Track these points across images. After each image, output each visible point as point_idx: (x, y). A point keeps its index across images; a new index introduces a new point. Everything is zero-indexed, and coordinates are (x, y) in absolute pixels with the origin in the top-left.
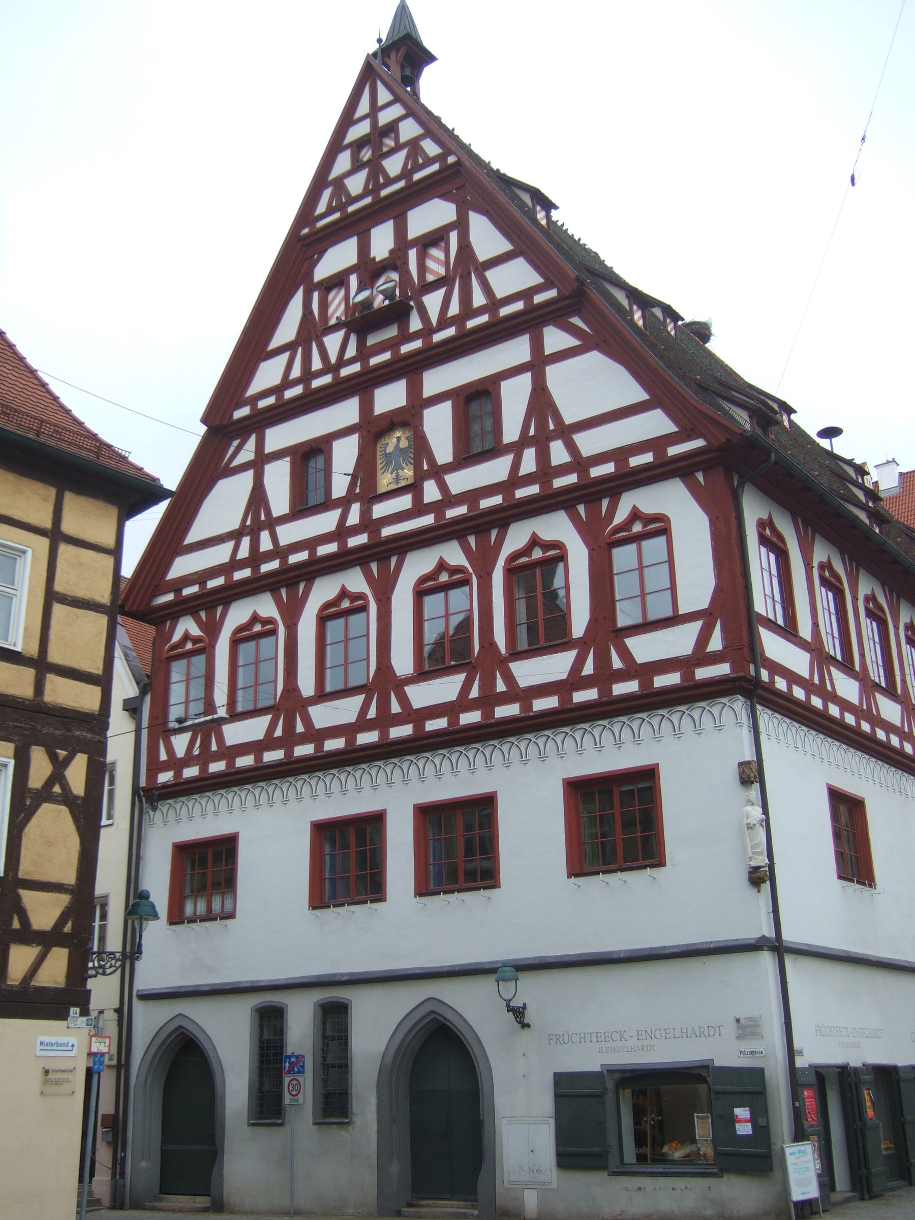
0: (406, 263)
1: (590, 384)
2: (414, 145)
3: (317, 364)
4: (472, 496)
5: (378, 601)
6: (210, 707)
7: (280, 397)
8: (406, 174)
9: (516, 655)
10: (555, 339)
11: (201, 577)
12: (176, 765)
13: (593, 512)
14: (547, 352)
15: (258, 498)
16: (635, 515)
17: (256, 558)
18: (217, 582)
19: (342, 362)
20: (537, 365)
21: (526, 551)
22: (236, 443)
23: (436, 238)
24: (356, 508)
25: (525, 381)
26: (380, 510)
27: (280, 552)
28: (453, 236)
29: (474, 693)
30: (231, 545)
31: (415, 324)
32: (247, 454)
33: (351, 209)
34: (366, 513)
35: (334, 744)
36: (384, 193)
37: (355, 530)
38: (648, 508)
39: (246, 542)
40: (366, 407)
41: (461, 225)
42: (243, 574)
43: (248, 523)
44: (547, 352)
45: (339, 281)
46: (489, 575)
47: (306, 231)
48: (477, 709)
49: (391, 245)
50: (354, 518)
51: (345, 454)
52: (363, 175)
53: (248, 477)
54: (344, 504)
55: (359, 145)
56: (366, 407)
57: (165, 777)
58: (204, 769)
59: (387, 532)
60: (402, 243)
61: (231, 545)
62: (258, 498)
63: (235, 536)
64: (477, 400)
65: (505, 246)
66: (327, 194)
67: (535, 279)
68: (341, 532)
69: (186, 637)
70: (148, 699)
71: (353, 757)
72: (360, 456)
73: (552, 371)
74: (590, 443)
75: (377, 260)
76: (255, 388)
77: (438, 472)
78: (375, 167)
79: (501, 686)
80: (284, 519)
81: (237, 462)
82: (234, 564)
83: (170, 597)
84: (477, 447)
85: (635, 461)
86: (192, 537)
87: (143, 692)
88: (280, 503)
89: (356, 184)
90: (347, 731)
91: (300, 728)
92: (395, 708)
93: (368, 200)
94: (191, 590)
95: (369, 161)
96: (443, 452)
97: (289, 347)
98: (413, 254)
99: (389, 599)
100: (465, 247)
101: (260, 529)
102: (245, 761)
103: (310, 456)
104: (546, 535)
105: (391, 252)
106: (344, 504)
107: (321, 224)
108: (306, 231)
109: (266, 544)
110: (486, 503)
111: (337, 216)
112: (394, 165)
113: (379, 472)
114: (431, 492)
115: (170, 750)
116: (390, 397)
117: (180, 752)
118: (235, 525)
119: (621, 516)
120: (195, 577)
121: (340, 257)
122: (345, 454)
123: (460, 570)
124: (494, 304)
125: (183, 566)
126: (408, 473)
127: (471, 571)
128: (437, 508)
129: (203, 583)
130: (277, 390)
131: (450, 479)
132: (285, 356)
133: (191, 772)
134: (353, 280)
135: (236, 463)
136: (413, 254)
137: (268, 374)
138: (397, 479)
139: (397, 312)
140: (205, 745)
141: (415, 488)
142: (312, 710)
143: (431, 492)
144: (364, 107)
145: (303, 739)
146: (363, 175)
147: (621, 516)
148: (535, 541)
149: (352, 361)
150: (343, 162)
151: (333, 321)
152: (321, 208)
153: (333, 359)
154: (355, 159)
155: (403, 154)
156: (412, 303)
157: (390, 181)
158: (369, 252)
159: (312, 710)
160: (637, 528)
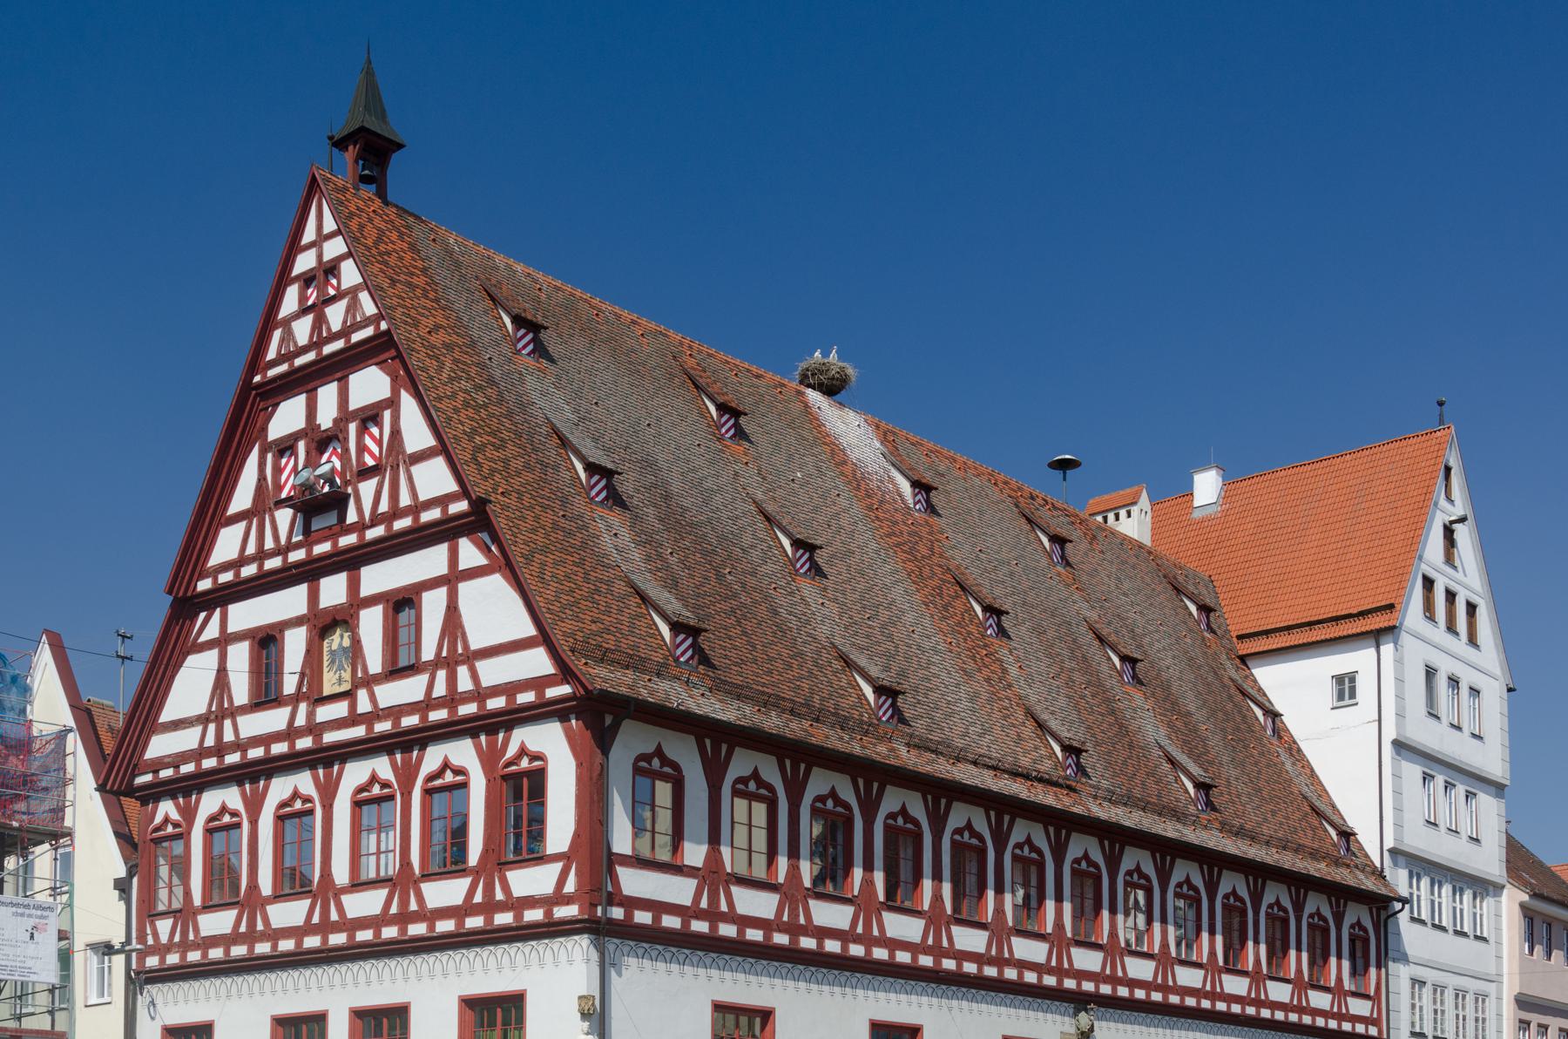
0: (346, 439)
1: (494, 611)
2: (353, 292)
3: (269, 544)
4: (396, 712)
5: (324, 806)
6: (188, 894)
7: (237, 574)
8: (345, 332)
9: (427, 876)
10: (470, 554)
11: (177, 760)
12: (162, 950)
13: (492, 745)
14: (462, 567)
15: (222, 682)
16: (523, 751)
17: (220, 750)
19: (291, 547)
20: (453, 578)
22: (203, 615)
23: (370, 416)
24: (303, 707)
25: (441, 593)
26: (325, 713)
27: (240, 746)
28: (387, 414)
29: (394, 910)
30: (199, 729)
32: (212, 632)
33: (299, 362)
34: (311, 715)
35: (287, 945)
36: (328, 349)
37: (301, 732)
38: (533, 747)
39: (212, 727)
40: (313, 596)
41: (393, 403)
42: (209, 763)
44: (462, 567)
45: (285, 447)
46: (410, 793)
47: (257, 379)
48: (395, 924)
50: (301, 721)
51: (295, 644)
52: (308, 320)
53: (212, 656)
54: (295, 699)
56: (313, 596)
57: (152, 962)
58: (183, 957)
59: (330, 737)
61: (199, 729)
62: (222, 682)
63: (203, 720)
65: (430, 441)
66: (277, 334)
67: (452, 487)
68: (290, 734)
69: (166, 820)
70: (135, 880)
71: (300, 960)
72: (308, 651)
73: (464, 588)
74: (493, 672)
76: (215, 559)
77: (369, 682)
78: (317, 310)
79: (413, 906)
80: (244, 710)
81: (202, 639)
82: (200, 753)
83: (147, 778)
84: (403, 661)
86: (165, 717)
87: (130, 875)
88: (241, 692)
89: (302, 330)
90: (297, 933)
91: (260, 926)
92: (334, 916)
93: (311, 356)
94: (166, 773)
95: (314, 305)
96: (375, 664)
98: (353, 428)
99: (331, 806)
100: (396, 433)
101: (223, 718)
102: (216, 953)
104: (456, 761)
105: (335, 421)
106: (295, 699)
107: (272, 373)
108: (257, 379)
109: (229, 736)
110: (410, 721)
111: (284, 368)
112: (336, 315)
113: (325, 670)
114: (364, 705)
115: (156, 935)
116: (333, 590)
117: (164, 939)
118: (203, 710)
119: (512, 751)
121: (287, 418)
122: (295, 644)
123: (385, 785)
124: (417, 508)
125: (159, 746)
126: (347, 675)
128: (370, 719)
129: (177, 767)
131: (378, 689)
132: (243, 524)
133: (173, 959)
134: (301, 446)
135: (202, 639)
136: (353, 428)
137: (227, 544)
138: (340, 680)
139: (337, 501)
140: (184, 933)
141: (349, 695)
142: (270, 909)
144: (309, 235)
145: (264, 937)
146: (308, 320)
147: (512, 751)
148: (446, 765)
149: (298, 546)
150: (290, 301)
151: (284, 495)
152: (271, 354)
153: (283, 541)
154: (303, 298)
155: (343, 304)
156: (350, 490)
157: (333, 337)
158: (315, 417)
159: (270, 909)
160: (525, 763)
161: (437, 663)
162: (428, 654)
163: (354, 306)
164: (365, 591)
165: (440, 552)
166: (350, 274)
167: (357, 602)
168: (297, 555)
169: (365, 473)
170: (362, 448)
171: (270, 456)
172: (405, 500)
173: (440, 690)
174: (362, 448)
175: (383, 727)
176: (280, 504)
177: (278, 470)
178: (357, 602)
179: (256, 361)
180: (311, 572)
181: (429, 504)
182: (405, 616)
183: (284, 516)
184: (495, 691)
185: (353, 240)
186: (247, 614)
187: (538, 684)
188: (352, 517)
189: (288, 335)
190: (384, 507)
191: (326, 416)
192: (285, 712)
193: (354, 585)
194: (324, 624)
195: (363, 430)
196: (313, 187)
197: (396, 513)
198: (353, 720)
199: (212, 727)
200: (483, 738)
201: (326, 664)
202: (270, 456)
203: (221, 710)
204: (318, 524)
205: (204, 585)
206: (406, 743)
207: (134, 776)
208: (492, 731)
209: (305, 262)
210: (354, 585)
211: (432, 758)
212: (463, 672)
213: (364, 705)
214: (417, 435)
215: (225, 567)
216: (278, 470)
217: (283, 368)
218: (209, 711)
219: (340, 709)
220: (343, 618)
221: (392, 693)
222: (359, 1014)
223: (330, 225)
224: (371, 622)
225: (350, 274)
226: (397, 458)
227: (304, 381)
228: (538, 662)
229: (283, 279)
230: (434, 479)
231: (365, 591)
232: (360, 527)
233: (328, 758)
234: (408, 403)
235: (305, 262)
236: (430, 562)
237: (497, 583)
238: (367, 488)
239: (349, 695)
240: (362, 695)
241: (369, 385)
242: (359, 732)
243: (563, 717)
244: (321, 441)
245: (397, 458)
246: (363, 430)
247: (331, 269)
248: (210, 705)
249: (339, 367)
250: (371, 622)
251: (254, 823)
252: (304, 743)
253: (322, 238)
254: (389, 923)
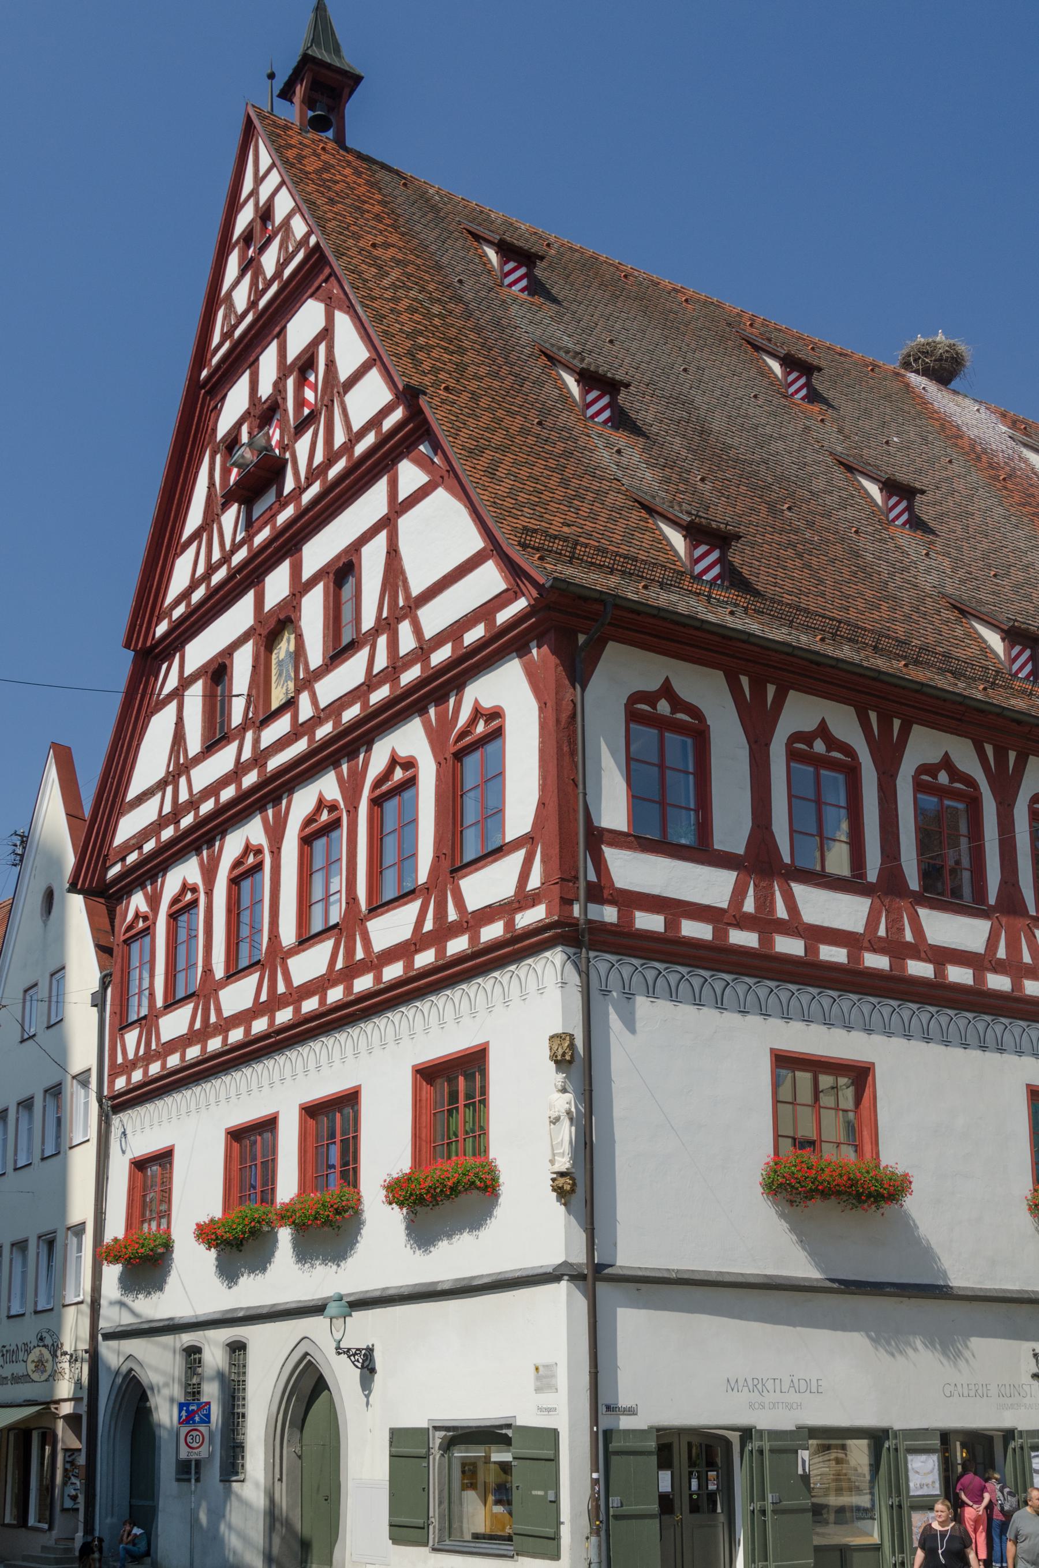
3: (216, 555)
11: (137, 842)
13: (441, 717)
16: (477, 713)
18: (149, 846)
22: (165, 666)
24: (249, 735)
27: (193, 804)
31: (289, 485)
38: (487, 704)
39: (169, 790)
43: (171, 769)
46: (356, 808)
49: (273, 376)
59: (274, 763)
63: (161, 786)
75: (263, 399)
94: (132, 858)
96: (315, 657)
97: (196, 535)
98: (290, 382)
101: (179, 775)
103: (218, 672)
104: (403, 753)
113: (273, 685)
114: (306, 711)
118: (161, 774)
120: (133, 842)
121: (236, 402)
125: (128, 827)
126: (291, 685)
127: (342, 806)
129: (140, 848)
130: (186, 595)
136: (290, 382)
143: (306, 711)
148: (394, 761)
156: (287, 455)
160: (480, 728)
169: (300, 429)
171: (218, 457)
174: (300, 402)
176: (225, 507)
178: (299, 588)
180: (249, 577)
186: (199, 651)
193: (296, 570)
195: (302, 381)
199: (169, 790)
200: (432, 711)
201: (274, 678)
202: (218, 457)
203: (180, 767)
205: (162, 629)
206: (348, 745)
207: (106, 869)
208: (439, 697)
210: (296, 570)
215: (177, 603)
218: (168, 773)
221: (332, 687)
222: (311, 1111)
224: (313, 608)
227: (243, 356)
231: (307, 574)
233: (271, 793)
240: (304, 699)
246: (302, 381)
248: (168, 766)
249: (270, 323)
250: (313, 608)
251: (209, 893)
254: (334, 984)
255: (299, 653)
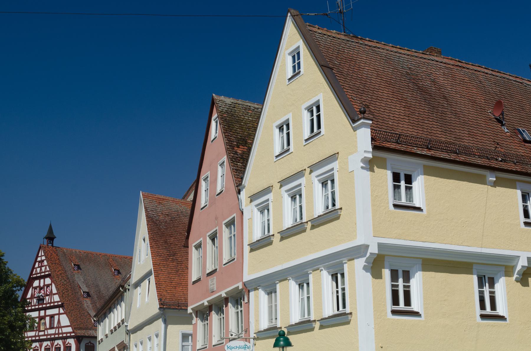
1: (65, 320)
2: (46, 266)
4: (51, 335)
16: (68, 343)
20: (59, 314)
21: (57, 345)
23: (48, 286)
41: (51, 284)
45: (35, 288)
50: (37, 334)
55: (39, 262)
59: (41, 338)
60: (44, 285)
64: (52, 317)
68: (35, 336)
74: (65, 330)
77: (47, 329)
78: (40, 267)
84: (52, 326)
85: (69, 335)
89: (38, 270)
96: (48, 326)
106: (36, 331)
110: (53, 336)
112: (43, 269)
116: (42, 313)
119: (67, 343)
121: (36, 283)
124: (54, 302)
139: (43, 300)
144: (40, 255)
147: (67, 343)
148: (58, 344)
150: (37, 265)
154: (39, 265)
157: (43, 272)
161: (57, 328)
162: (55, 326)
163: (46, 268)
164: (47, 314)
165: (58, 309)
166: (45, 263)
167: (46, 316)
168: (37, 307)
169: (47, 295)
170: (47, 291)
172: (52, 301)
173: (57, 332)
174: (47, 291)
175: (49, 337)
177: (35, 292)
179: (31, 274)
180: (39, 310)
181: (56, 302)
182: (52, 319)
183: (35, 300)
184: (65, 333)
185: (46, 257)
187: (70, 333)
188: (45, 302)
189: (36, 271)
190: (49, 301)
191: (42, 285)
192: (35, 332)
193: (45, 313)
194: (41, 318)
195: (47, 288)
196: (40, 248)
197: (51, 303)
198: (44, 335)
204: (40, 302)
206: (52, 340)
209: (39, 259)
210: (45, 313)
211: (56, 342)
212: (60, 329)
213: (46, 333)
214: (55, 291)
216: (35, 292)
217: (35, 276)
219: (42, 333)
220: (43, 318)
223: (43, 254)
225: (45, 263)
226: (51, 294)
227: (39, 278)
228: (70, 329)
229: (36, 261)
230: (56, 298)
231: (47, 314)
232: (46, 304)
234: (53, 285)
235: (39, 259)
236: (55, 311)
237: (65, 316)
238: (47, 297)
239: (44, 331)
240: (46, 331)
241: (48, 281)
242: (45, 337)
243: (74, 338)
244: (41, 288)
245: (51, 294)
246: (47, 288)
247: (42, 261)
249: (44, 277)
250: (48, 319)
252: (37, 338)
253: (41, 256)
255: (45, 323)
